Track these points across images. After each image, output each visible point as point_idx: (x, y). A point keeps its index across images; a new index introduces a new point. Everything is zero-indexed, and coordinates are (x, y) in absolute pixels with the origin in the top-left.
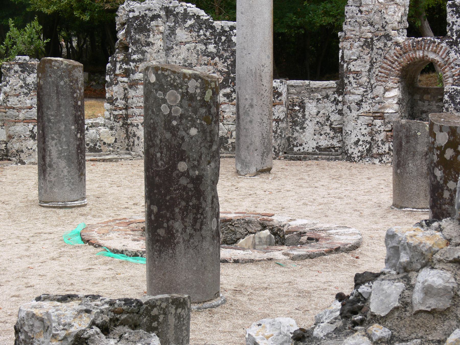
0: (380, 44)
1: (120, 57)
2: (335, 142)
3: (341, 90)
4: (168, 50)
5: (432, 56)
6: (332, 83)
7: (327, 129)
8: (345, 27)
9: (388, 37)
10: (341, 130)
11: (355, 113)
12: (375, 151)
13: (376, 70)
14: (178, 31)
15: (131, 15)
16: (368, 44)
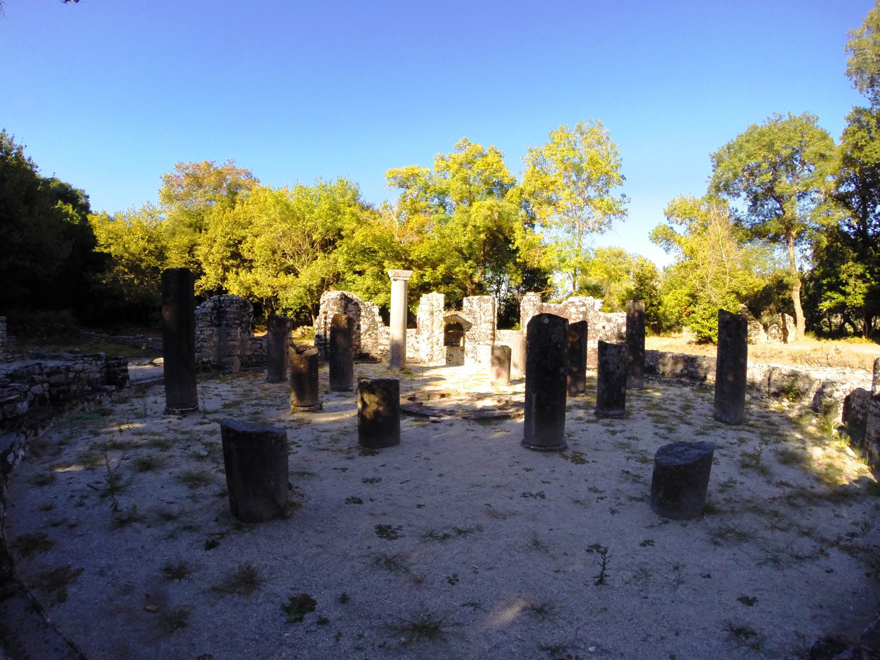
6: (414, 330)
7: (412, 349)
9: (440, 311)
12: (435, 358)
13: (435, 324)
16: (432, 313)
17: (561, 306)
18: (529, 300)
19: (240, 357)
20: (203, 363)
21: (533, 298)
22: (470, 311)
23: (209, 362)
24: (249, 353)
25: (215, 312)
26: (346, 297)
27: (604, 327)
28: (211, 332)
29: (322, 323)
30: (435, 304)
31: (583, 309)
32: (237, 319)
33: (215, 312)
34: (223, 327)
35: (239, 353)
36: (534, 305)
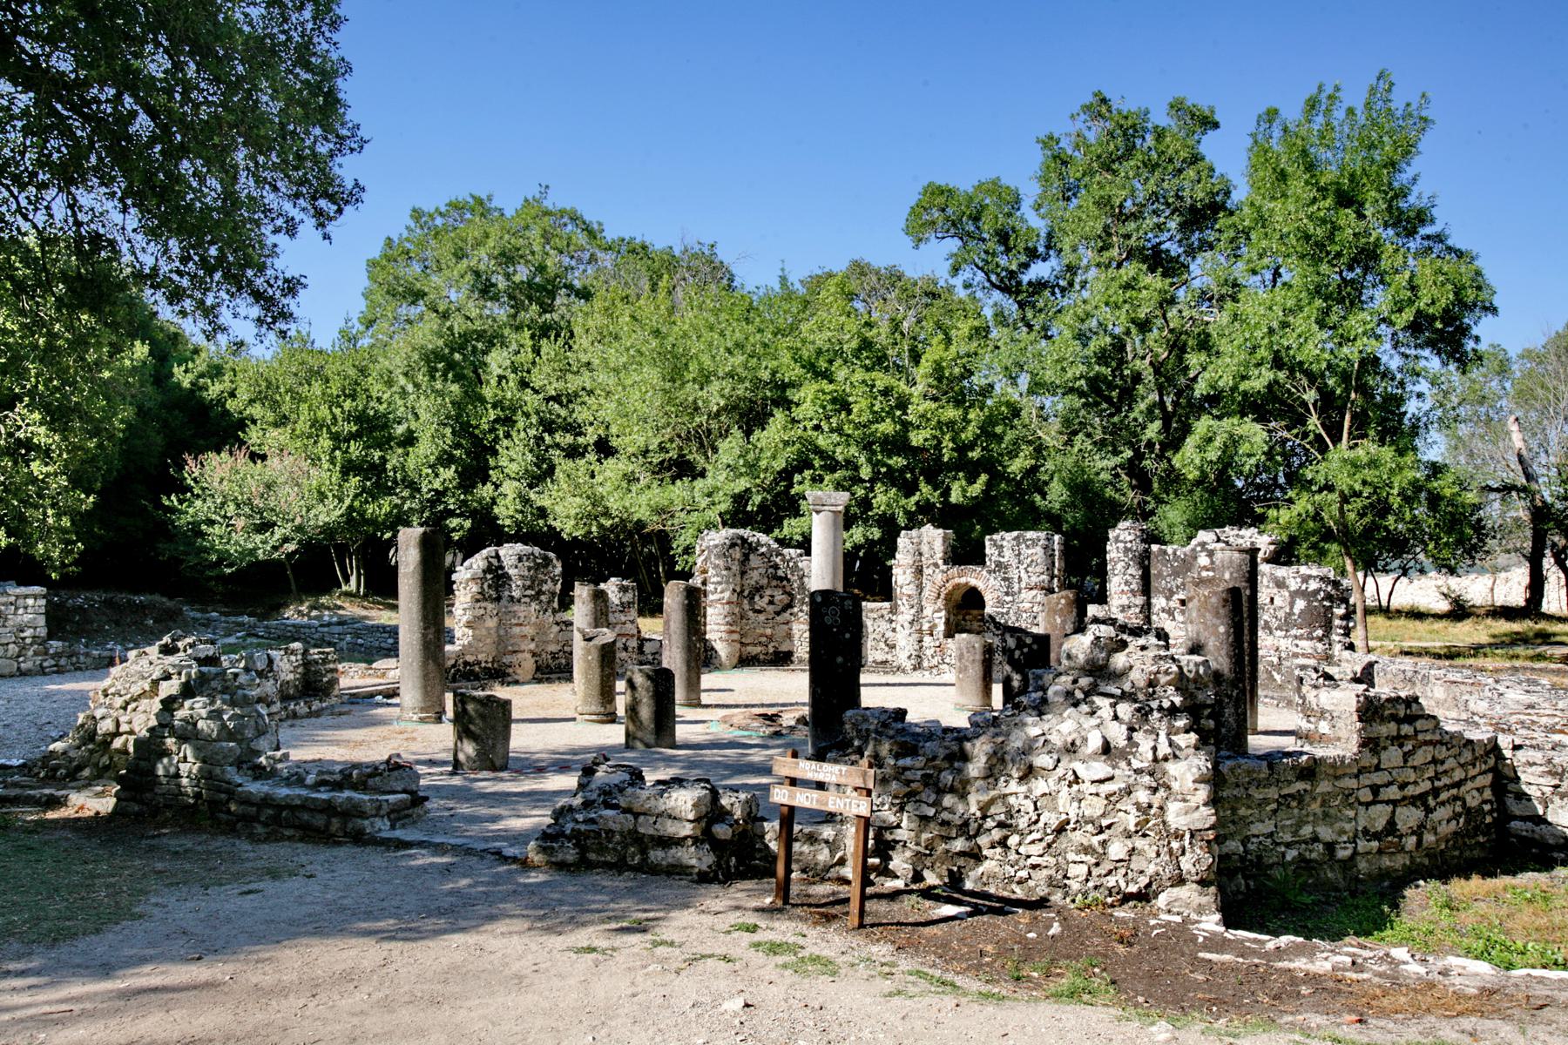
2: (889, 657)
3: (894, 610)
4: (743, 573)
5: (973, 582)
6: (887, 604)
7: (882, 645)
9: (936, 565)
10: (893, 647)
12: (925, 664)
13: (926, 593)
16: (919, 571)
19: (534, 654)
20: (466, 663)
22: (999, 564)
23: (479, 663)
24: (553, 648)
30: (925, 548)
32: (529, 588)
34: (504, 602)
35: (532, 646)
36: (1127, 550)
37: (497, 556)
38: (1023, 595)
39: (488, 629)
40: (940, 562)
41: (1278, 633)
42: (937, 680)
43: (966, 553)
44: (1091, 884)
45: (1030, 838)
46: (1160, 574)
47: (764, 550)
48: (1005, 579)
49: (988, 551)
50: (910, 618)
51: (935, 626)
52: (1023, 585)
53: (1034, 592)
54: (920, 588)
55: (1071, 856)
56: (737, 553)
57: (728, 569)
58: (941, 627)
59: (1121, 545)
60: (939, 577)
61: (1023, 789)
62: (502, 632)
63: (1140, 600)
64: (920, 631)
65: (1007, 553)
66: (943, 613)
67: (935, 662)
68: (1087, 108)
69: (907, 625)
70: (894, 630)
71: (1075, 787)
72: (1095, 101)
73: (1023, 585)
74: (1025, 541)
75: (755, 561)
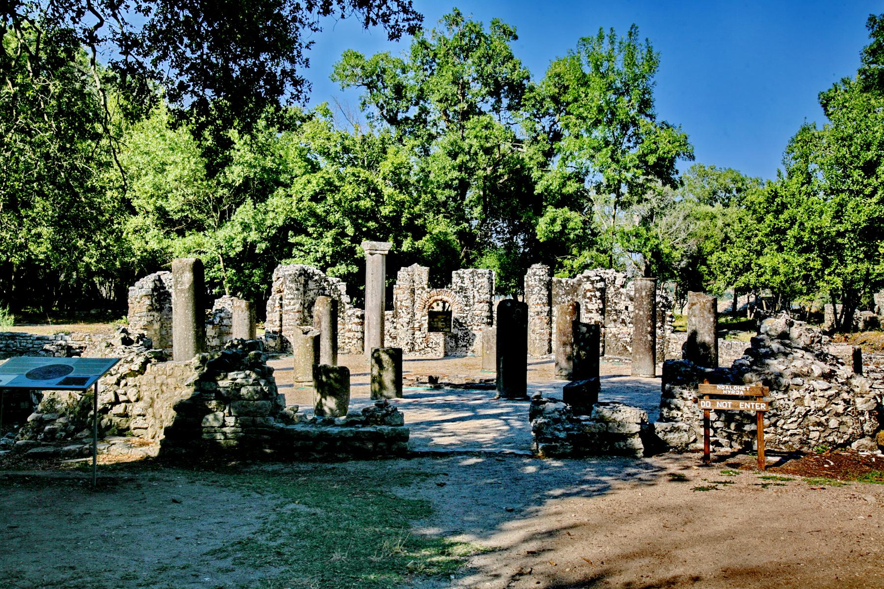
0: (419, 292)
1: (278, 296)
4: (305, 292)
8: (397, 282)
9: (423, 288)
10: (395, 338)
11: (406, 329)
12: (417, 348)
13: (417, 305)
14: (310, 282)
15: (287, 273)
17: (575, 280)
18: (534, 274)
21: (539, 272)
22: (461, 288)
25: (155, 294)
26: (306, 272)
27: (627, 308)
28: (152, 318)
29: (277, 305)
30: (416, 278)
31: (600, 285)
33: (155, 294)
34: (165, 311)
36: (541, 280)
37: (160, 280)
38: (477, 306)
39: (155, 330)
40: (426, 287)
41: (631, 325)
42: (424, 357)
43: (440, 278)
44: (821, 441)
45: (789, 421)
46: (557, 293)
47: (317, 278)
48: (465, 297)
49: (454, 280)
50: (407, 320)
51: (422, 325)
52: (476, 300)
53: (482, 304)
54: (413, 302)
55: (811, 428)
56: (302, 279)
57: (298, 290)
58: (426, 326)
59: (537, 277)
60: (425, 296)
61: (786, 396)
62: (164, 332)
63: (547, 308)
64: (413, 328)
65: (466, 281)
66: (427, 317)
67: (422, 346)
68: (447, 18)
69: (405, 324)
70: (395, 328)
71: (812, 393)
72: (453, 14)
73: (476, 300)
74: (477, 274)
75: (311, 285)
